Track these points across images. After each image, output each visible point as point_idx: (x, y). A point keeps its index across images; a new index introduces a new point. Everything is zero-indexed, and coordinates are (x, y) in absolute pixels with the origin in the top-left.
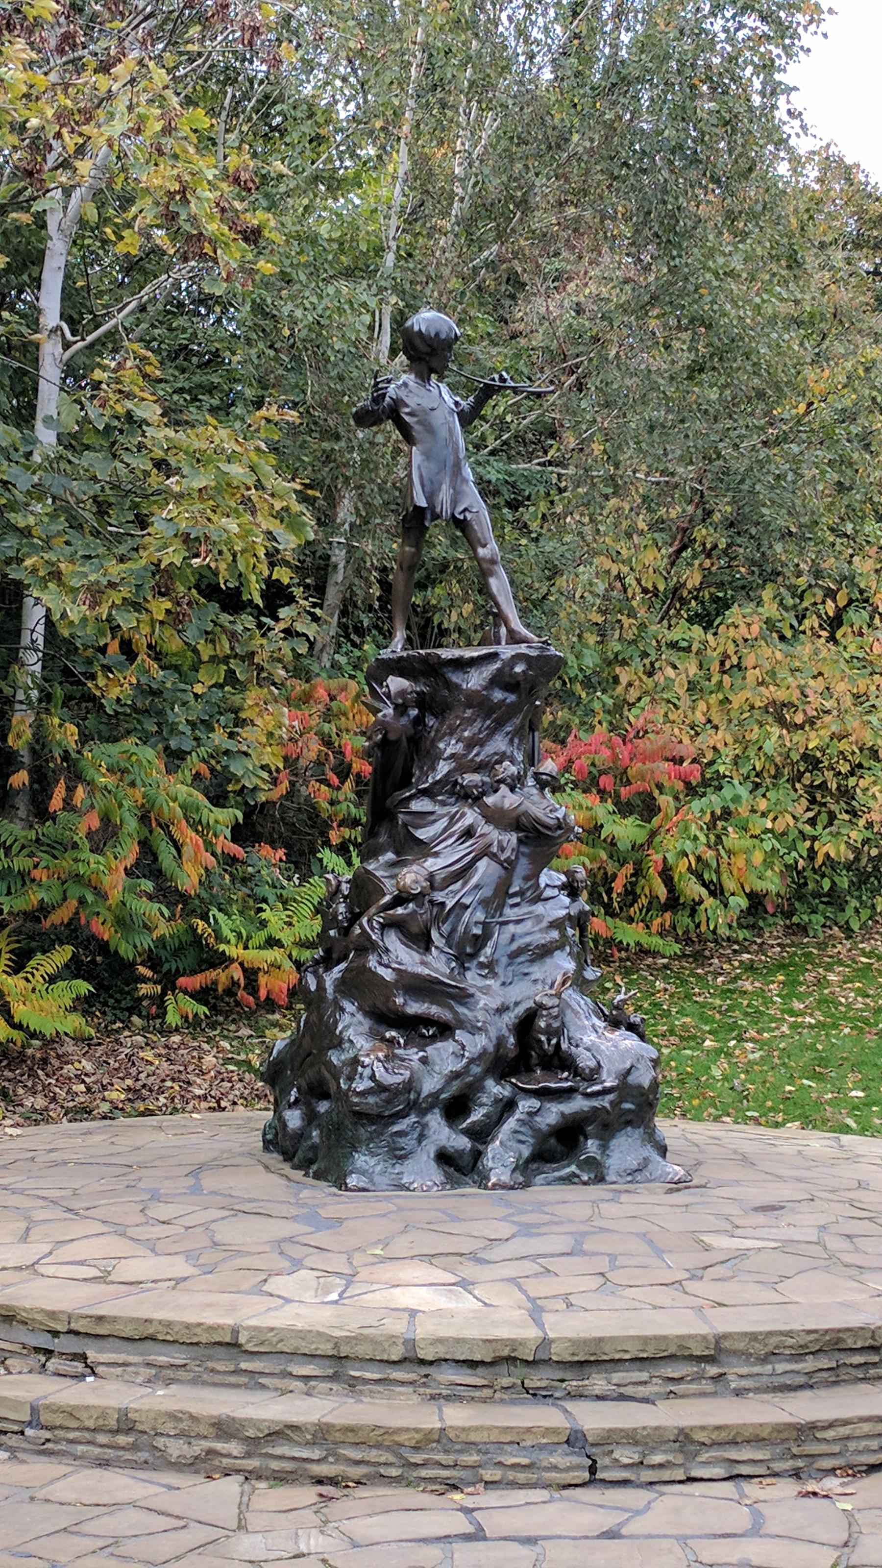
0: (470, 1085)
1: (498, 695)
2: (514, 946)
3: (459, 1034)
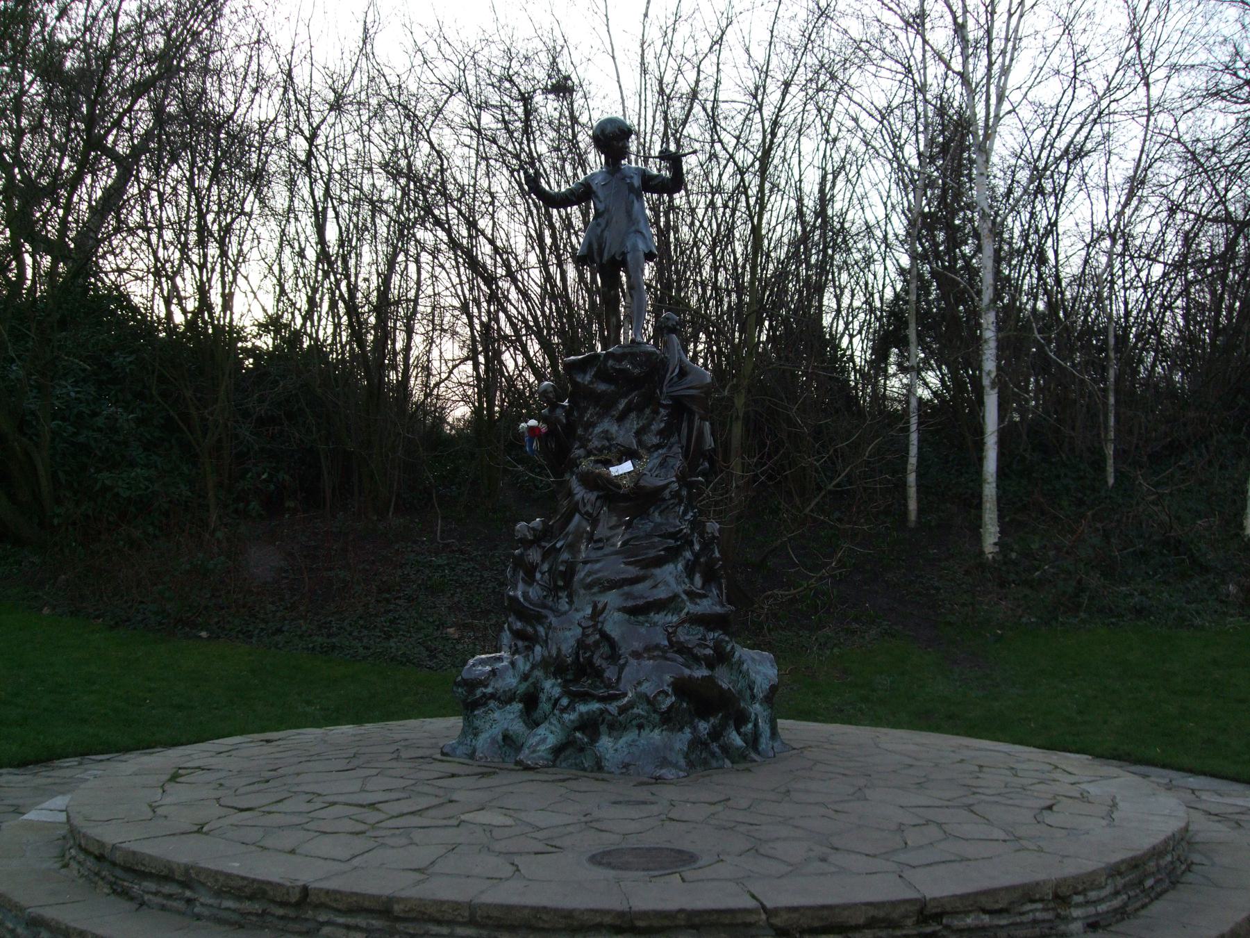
0: (535, 685)
1: (602, 387)
2: (589, 580)
3: (538, 648)
